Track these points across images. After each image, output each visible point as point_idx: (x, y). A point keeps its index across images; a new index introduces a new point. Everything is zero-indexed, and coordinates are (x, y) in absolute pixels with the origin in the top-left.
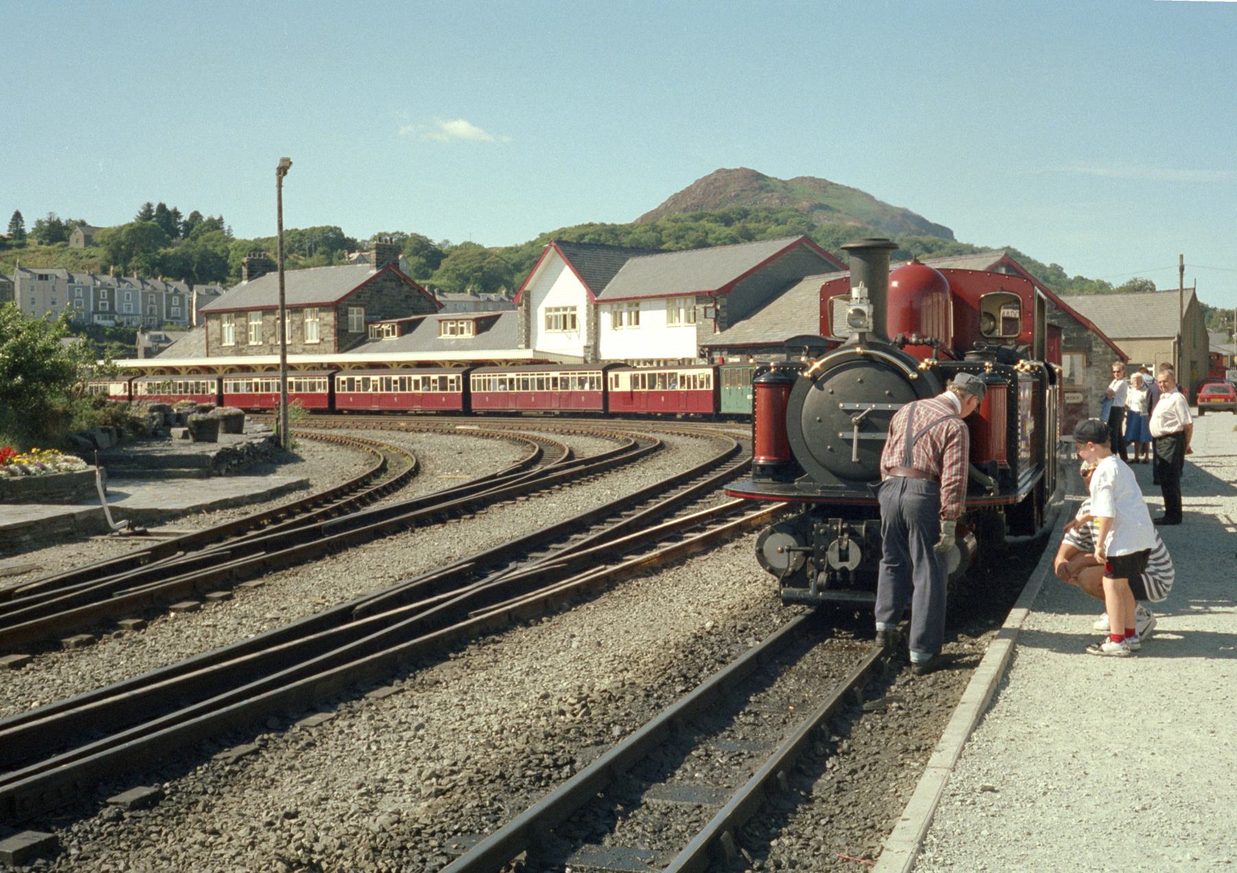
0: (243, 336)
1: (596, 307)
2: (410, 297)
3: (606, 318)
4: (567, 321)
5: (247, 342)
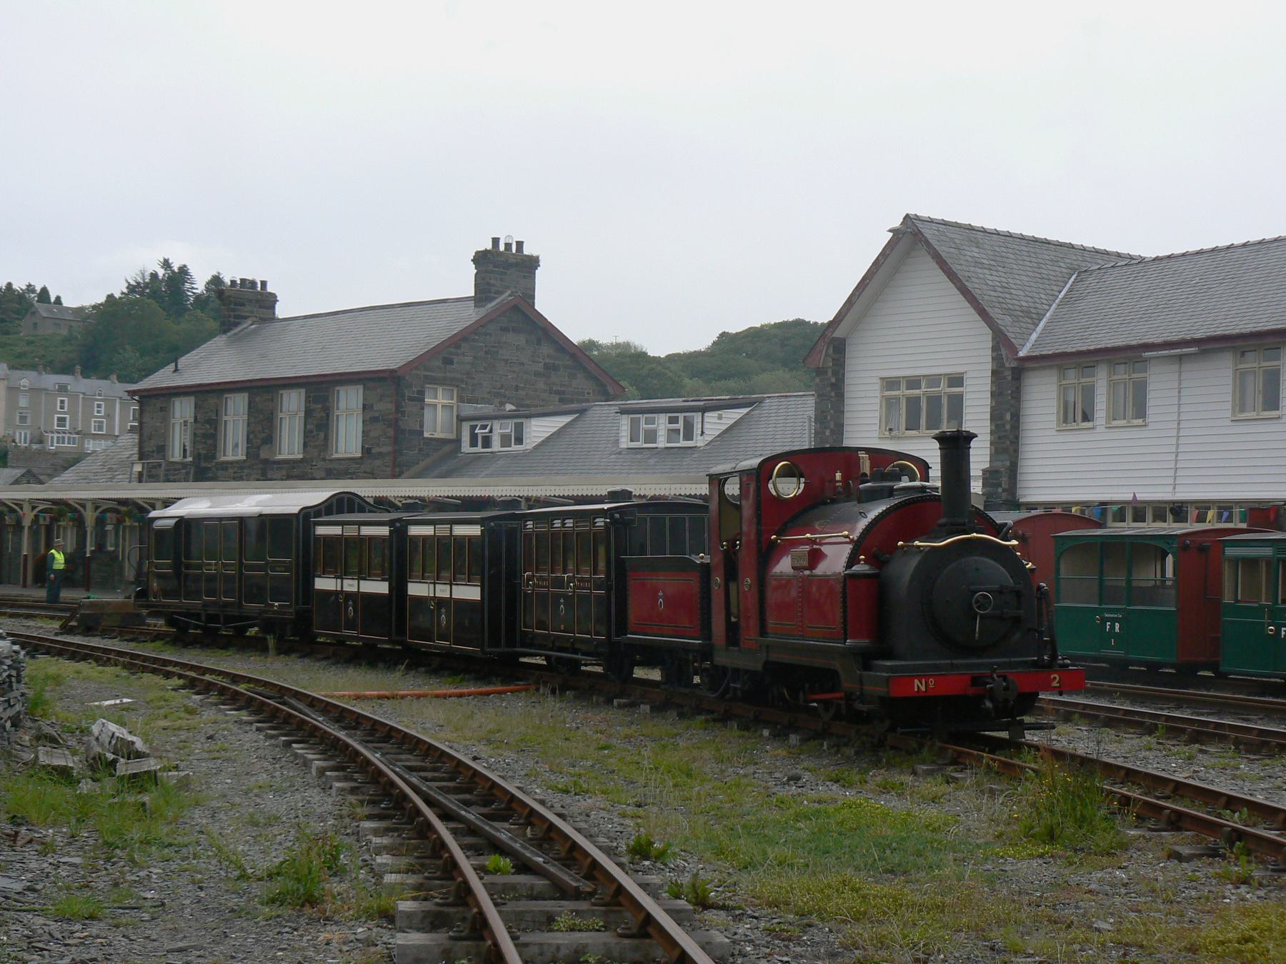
0: (210, 442)
2: (555, 368)
5: (214, 457)
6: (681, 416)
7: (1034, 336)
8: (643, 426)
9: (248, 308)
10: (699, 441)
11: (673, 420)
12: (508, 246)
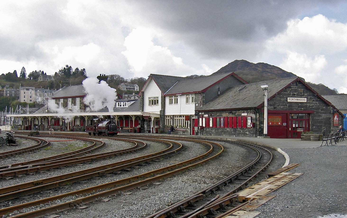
1: (165, 97)
3: (167, 100)
4: (154, 102)
6: (125, 102)
7: (167, 91)
8: (120, 104)
9: (64, 84)
10: (127, 106)
11: (123, 103)
12: (103, 75)
